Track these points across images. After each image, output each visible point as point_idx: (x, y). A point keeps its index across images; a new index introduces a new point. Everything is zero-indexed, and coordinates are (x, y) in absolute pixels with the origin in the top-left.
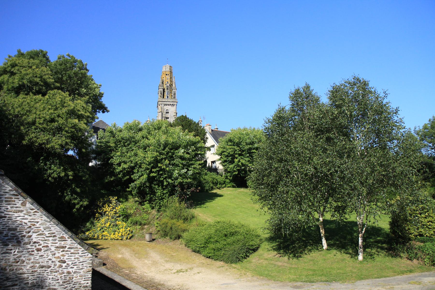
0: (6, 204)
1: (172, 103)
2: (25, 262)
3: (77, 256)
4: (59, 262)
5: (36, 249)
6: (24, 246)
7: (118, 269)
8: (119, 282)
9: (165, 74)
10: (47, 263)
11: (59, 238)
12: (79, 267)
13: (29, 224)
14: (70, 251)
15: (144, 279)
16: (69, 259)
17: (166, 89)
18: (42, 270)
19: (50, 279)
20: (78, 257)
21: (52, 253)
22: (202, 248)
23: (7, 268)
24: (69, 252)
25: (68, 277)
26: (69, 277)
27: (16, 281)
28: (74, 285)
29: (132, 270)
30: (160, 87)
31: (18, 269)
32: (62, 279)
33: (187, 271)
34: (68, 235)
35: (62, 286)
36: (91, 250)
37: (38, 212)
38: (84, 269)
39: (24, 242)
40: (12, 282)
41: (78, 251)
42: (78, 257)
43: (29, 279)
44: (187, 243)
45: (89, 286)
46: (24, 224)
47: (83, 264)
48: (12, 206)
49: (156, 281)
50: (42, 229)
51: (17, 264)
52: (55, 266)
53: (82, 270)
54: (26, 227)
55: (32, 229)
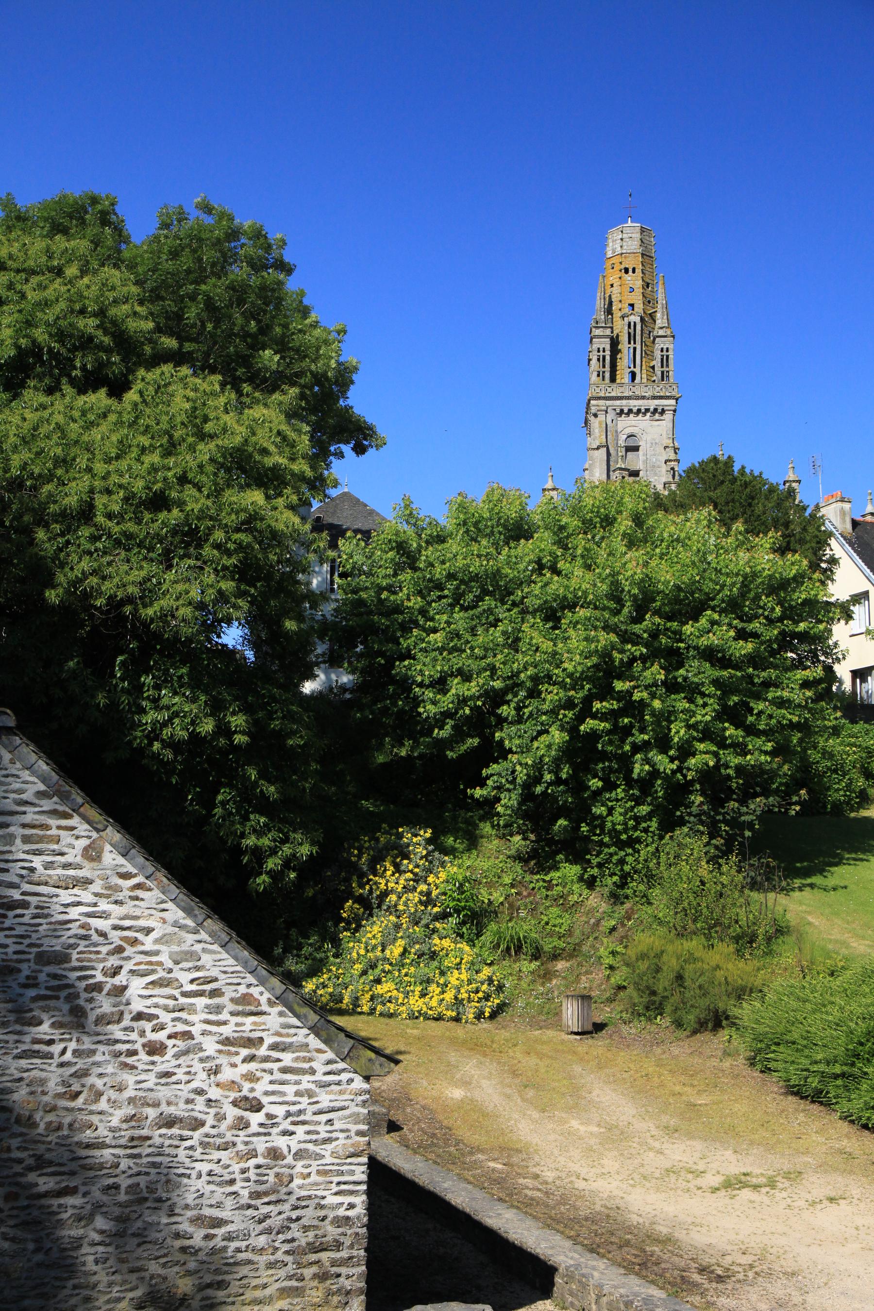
0: (27, 852)
1: (652, 404)
2: (104, 1099)
3: (306, 1081)
4: (235, 1103)
5: (144, 1046)
6: (99, 1029)
7: (452, 1149)
8: (468, 1210)
9: (617, 267)
10: (190, 1106)
11: (232, 1000)
12: (318, 1133)
13: (115, 936)
14: (279, 1060)
15: (576, 1209)
16: (273, 1093)
17: (624, 338)
18: (170, 1138)
19: (199, 1176)
20: (312, 1086)
21: (208, 1065)
22: (839, 1082)
23: (37, 1117)
24: (276, 1066)
25: (272, 1173)
26: (277, 1175)
27: (73, 1173)
28: (295, 1208)
29: (515, 1159)
30: (597, 332)
31: (77, 1125)
32: (248, 1180)
33: (772, 1184)
34: (271, 990)
35: (250, 1212)
36: (363, 1061)
37: (150, 890)
38: (334, 1144)
39: (99, 1011)
40: (58, 1178)
41: (311, 1060)
42: (312, 1086)
43: (118, 1171)
44: (760, 1050)
45: (358, 1218)
46: (95, 938)
47: (330, 1122)
48: (49, 859)
49: (635, 1219)
50: (164, 958)
51: (72, 1104)
52: (219, 1121)
53: (330, 1147)
54: (104, 949)
55: (128, 958)
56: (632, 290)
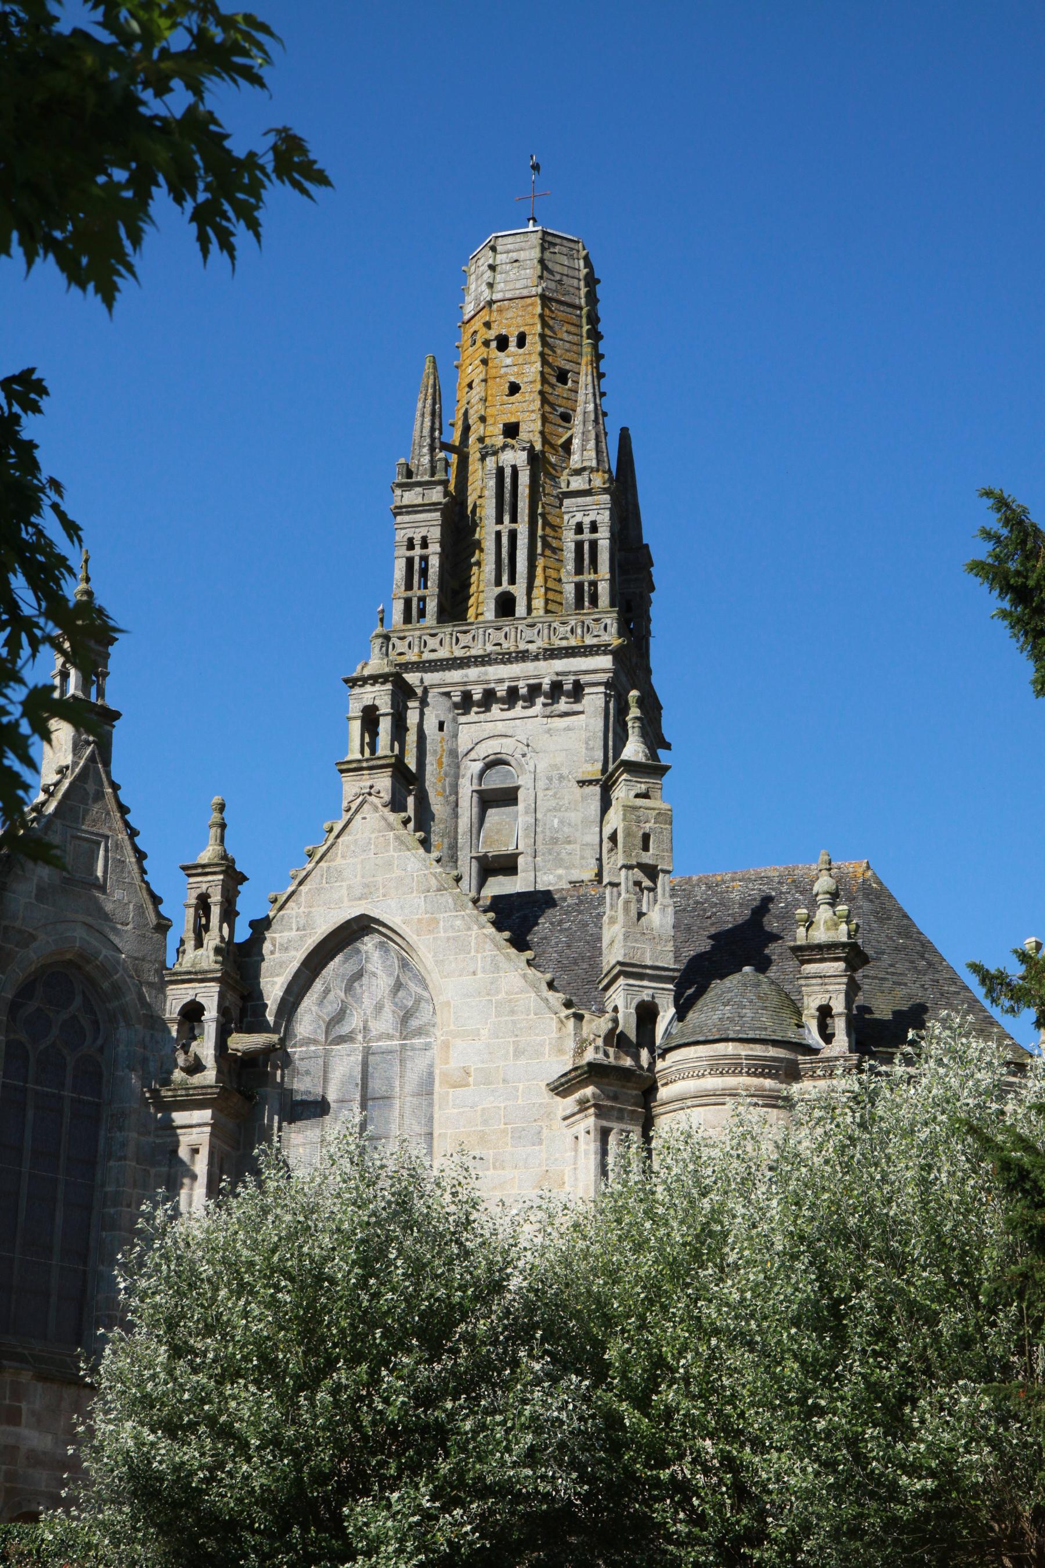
1: (547, 671)
30: (411, 497)
56: (514, 389)
